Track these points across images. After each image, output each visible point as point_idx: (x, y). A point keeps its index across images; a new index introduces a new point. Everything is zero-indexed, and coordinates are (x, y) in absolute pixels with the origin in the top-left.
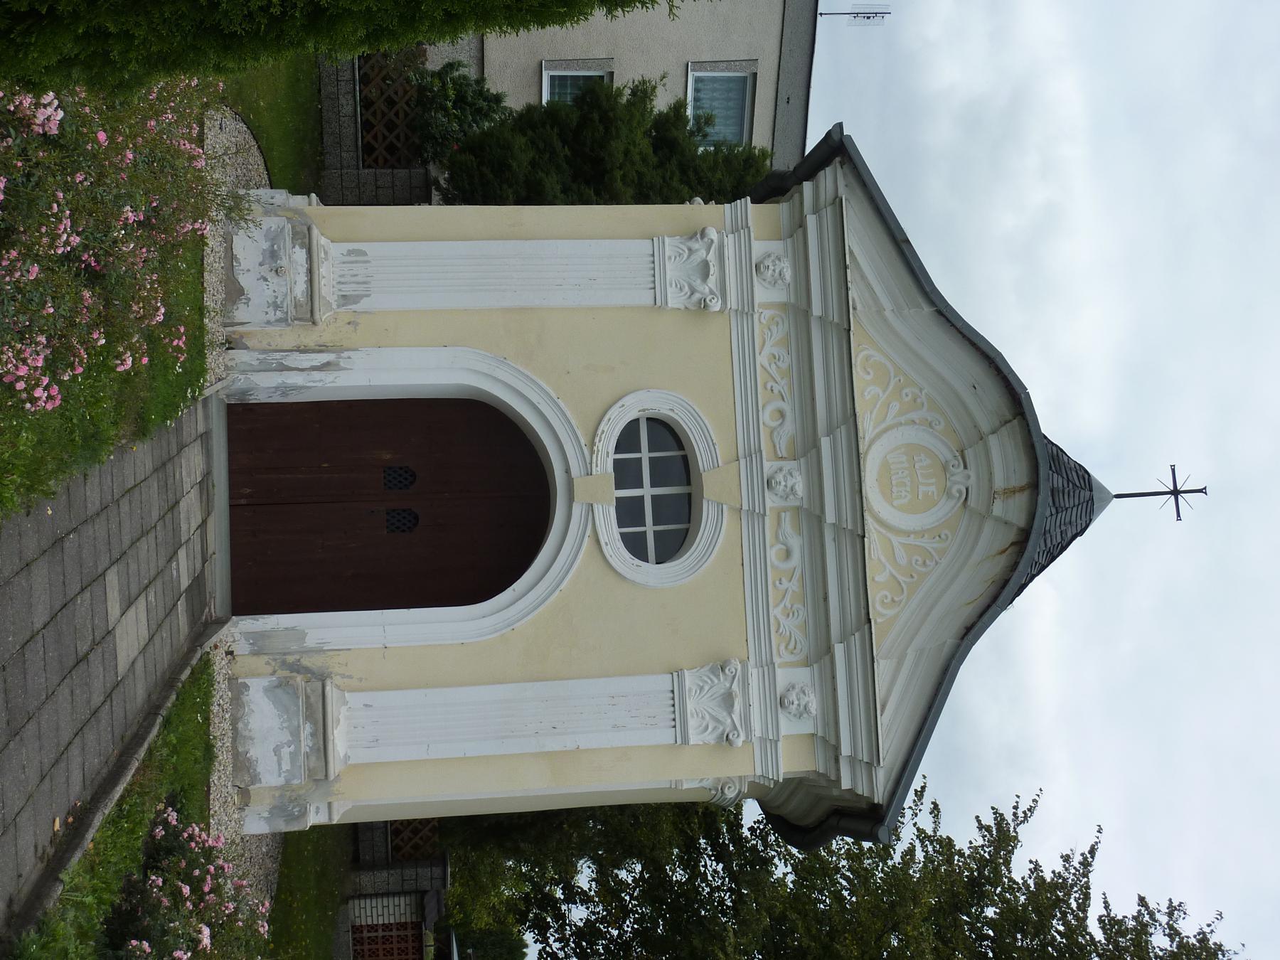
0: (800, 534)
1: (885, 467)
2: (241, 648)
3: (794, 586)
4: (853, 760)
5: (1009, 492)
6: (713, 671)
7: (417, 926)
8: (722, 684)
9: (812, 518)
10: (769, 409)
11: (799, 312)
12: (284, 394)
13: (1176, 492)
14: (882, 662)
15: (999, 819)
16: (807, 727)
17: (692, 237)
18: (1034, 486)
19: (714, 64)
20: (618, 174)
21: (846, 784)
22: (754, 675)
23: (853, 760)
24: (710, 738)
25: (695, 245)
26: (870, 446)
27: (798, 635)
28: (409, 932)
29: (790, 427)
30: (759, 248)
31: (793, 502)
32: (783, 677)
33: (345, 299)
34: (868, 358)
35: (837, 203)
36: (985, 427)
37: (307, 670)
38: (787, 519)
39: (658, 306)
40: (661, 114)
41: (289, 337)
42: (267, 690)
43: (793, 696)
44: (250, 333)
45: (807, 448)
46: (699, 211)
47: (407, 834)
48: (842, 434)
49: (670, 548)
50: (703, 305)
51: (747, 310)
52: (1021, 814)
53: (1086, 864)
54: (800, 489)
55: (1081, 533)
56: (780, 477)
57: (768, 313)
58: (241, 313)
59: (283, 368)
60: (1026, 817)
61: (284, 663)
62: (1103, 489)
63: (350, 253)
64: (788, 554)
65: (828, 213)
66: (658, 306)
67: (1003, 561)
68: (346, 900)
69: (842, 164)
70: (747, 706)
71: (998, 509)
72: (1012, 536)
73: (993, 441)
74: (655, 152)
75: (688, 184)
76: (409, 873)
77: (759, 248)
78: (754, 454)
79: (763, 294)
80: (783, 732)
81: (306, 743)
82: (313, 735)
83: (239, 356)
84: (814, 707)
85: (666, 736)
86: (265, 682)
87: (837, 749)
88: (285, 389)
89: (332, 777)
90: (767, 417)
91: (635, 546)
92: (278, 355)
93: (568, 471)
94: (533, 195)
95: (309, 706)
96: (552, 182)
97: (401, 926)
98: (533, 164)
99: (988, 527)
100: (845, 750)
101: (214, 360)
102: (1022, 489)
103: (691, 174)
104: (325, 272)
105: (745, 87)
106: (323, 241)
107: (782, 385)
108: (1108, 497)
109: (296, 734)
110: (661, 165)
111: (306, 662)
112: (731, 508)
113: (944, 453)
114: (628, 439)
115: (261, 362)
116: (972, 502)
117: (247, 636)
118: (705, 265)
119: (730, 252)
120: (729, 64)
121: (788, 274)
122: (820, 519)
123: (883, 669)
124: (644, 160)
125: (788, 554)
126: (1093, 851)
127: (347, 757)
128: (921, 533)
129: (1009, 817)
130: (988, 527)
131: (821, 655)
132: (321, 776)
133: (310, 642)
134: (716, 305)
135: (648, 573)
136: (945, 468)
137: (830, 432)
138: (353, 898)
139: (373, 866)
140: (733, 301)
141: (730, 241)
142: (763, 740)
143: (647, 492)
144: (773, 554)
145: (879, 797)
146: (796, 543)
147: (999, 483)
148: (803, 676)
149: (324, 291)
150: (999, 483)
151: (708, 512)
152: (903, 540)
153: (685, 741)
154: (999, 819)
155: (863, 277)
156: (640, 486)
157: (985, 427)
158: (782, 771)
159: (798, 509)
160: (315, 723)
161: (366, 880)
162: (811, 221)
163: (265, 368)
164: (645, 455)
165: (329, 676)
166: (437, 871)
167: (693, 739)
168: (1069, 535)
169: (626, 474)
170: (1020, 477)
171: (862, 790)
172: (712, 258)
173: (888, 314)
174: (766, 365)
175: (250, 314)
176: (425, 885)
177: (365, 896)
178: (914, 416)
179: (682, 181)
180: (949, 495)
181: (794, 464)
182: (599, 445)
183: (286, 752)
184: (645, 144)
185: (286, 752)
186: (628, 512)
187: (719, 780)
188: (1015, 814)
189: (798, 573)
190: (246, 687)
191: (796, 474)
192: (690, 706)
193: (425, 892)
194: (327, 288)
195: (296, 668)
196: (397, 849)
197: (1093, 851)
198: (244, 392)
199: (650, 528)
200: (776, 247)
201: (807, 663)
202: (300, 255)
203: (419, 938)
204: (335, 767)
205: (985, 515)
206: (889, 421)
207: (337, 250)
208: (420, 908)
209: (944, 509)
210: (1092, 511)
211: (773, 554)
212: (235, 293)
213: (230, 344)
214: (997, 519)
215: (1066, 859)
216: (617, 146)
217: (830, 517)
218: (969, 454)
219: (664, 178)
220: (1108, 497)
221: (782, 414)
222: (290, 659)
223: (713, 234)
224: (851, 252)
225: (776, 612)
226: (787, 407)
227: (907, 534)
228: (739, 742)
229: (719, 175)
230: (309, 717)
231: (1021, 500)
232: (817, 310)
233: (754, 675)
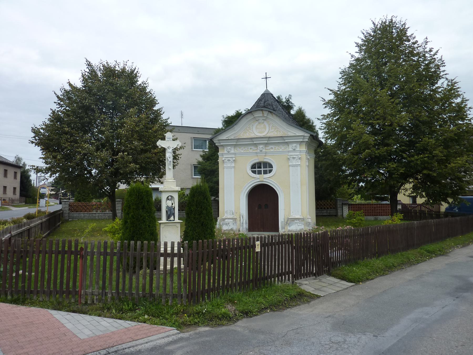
0: (269, 146)
1: (259, 133)
2: (284, 230)
3: (277, 147)
4: (303, 139)
5: (263, 114)
6: (289, 160)
7: (349, 205)
9: (266, 144)
10: (250, 150)
11: (235, 146)
12: (247, 223)
13: (266, 78)
15: (324, 104)
16: (298, 146)
18: (262, 110)
19: (192, 145)
20: (213, 168)
21: (307, 140)
22: (290, 154)
23: (303, 139)
24: (299, 161)
25: (225, 162)
27: (284, 147)
28: (350, 206)
29: (253, 147)
30: (226, 152)
32: (291, 149)
34: (242, 135)
36: (253, 117)
37: (287, 221)
38: (267, 148)
39: (234, 167)
40: (202, 159)
41: (238, 222)
42: (289, 227)
43: (293, 148)
44: (238, 228)
45: (256, 145)
46: (220, 160)
47: (318, 207)
48: (254, 140)
49: (271, 166)
50: (234, 160)
51: (235, 154)
52: (323, 100)
53: (331, 90)
54: (262, 146)
55: (272, 95)
56: (260, 149)
57: (235, 150)
58: (235, 229)
59: (243, 223)
60: (324, 99)
62: (265, 91)
63: (226, 213)
64: (272, 148)
65: (220, 141)
66: (234, 167)
67: (273, 115)
68: (343, 218)
70: (295, 155)
71: (266, 115)
72: (270, 113)
73: (255, 116)
74: (209, 161)
75: (215, 155)
76: (338, 206)
77: (226, 152)
78: (256, 153)
79: (232, 152)
80: (299, 150)
81: (298, 221)
82: (296, 220)
83: (241, 229)
84: (295, 145)
85: (299, 168)
86: (288, 227)
87: (301, 141)
88: (246, 223)
89: (303, 218)
90: (251, 151)
91: (270, 171)
93: (259, 182)
94: (217, 183)
95: (292, 221)
96: (215, 179)
97: (349, 208)
98: (211, 182)
99: (268, 117)
100: (302, 140)
101: (241, 232)
102: (263, 112)
103: (213, 155)
104: (229, 217)
105: (195, 139)
106: (224, 217)
107: (246, 148)
108: (267, 90)
109: (296, 223)
110: (211, 160)
111: (286, 221)
112: (265, 157)
113: (257, 123)
114: (254, 172)
115: (242, 226)
116: (265, 119)
117: (282, 230)
118: (228, 160)
119: (226, 156)
120: (192, 143)
121: (230, 147)
122: (267, 143)
124: (210, 163)
125: (272, 148)
126: (329, 89)
127: (300, 216)
128: (269, 127)
129: (324, 102)
130: (268, 117)
131: (287, 143)
132: (303, 219)
133: (283, 220)
134: (234, 159)
135: (274, 169)
136: (259, 123)
137: (253, 141)
138: (343, 216)
139: (337, 212)
140: (233, 156)
141: (225, 156)
142: (300, 152)
143: (262, 169)
144: (272, 150)
145: (309, 135)
146: (270, 147)
147: (262, 115)
148: (290, 146)
149: (232, 217)
150: (262, 115)
151: (265, 160)
152: (270, 130)
153: (300, 165)
154: (324, 104)
155: (230, 136)
157: (253, 117)
158: (305, 150)
159: (265, 146)
160: (295, 220)
161: (340, 214)
162: (221, 144)
163: (243, 226)
164: (257, 169)
165: (288, 218)
166: (338, 201)
167: (299, 163)
168: (273, 98)
169: (260, 173)
170: (261, 112)
171: (308, 138)
172: (227, 159)
173: (235, 132)
175: (235, 228)
176: (341, 203)
177: (343, 214)
178: (251, 128)
179: (214, 156)
180: (264, 122)
181: (258, 147)
182: (255, 177)
183: (299, 224)
184: (208, 163)
185: (299, 224)
186: (265, 172)
187: (306, 159)
188: (324, 101)
189: (275, 147)
190: (289, 230)
191: (260, 147)
192: (295, 164)
193: (342, 204)
194: (231, 216)
195: (287, 223)
196: (334, 208)
197: (329, 89)
198: (246, 229)
199: (268, 169)
200: (225, 149)
201: (289, 145)
202: (226, 220)
203: (352, 205)
204: (301, 217)
205: (267, 117)
206: (252, 132)
207: (226, 215)
208: (345, 204)
209: (265, 123)
210: (269, 93)
211: (272, 150)
212: (232, 230)
213: (239, 231)
214: (267, 115)
215: (330, 94)
216: (208, 168)
217: (266, 142)
218: (257, 119)
219: (213, 160)
220: (267, 90)
221: (251, 148)
222: (285, 223)
223: (223, 159)
226: (250, 148)
227: (269, 129)
228: (300, 156)
229: (213, 150)
231: (264, 112)
232: (235, 143)
233: (290, 154)
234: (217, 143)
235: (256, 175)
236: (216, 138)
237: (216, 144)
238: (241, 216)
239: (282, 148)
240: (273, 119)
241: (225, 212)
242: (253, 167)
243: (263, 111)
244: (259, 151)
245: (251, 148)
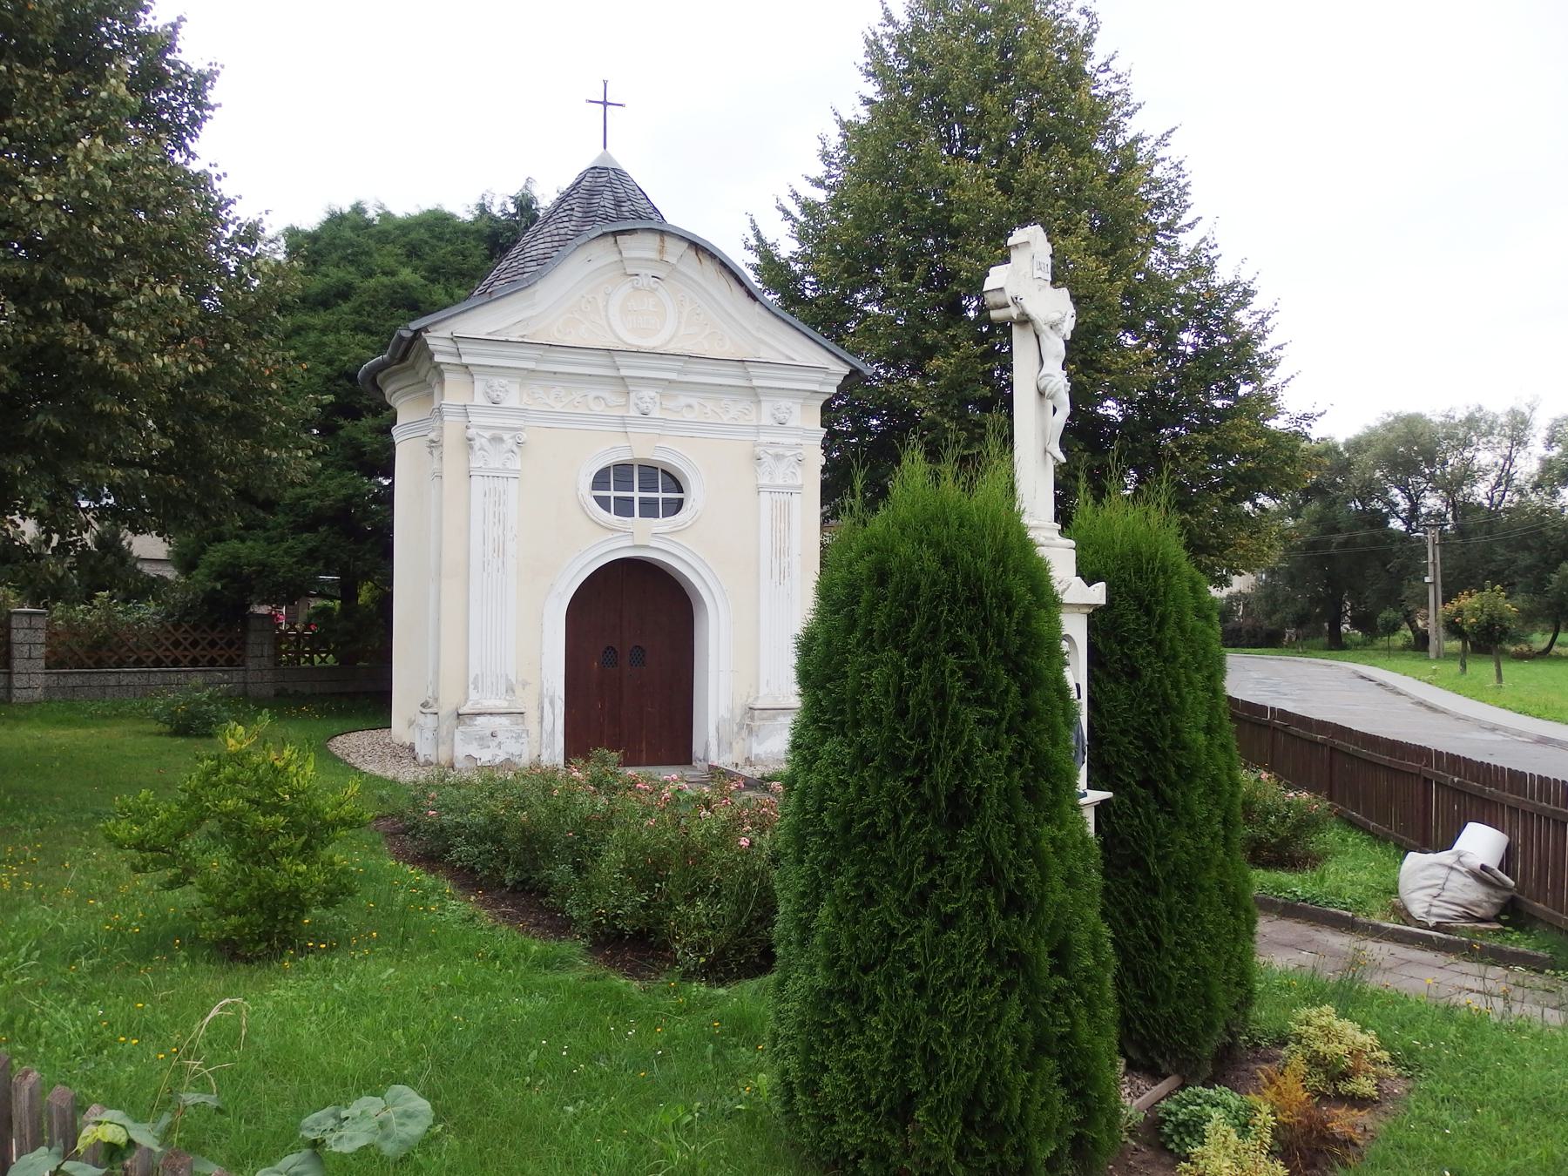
5: (661, 251)
6: (759, 466)
8: (767, 459)
13: (605, 103)
14: (761, 354)
16: (797, 409)
17: (471, 447)
23: (822, 383)
24: (799, 471)
25: (476, 447)
26: (620, 339)
31: (657, 399)
33: (510, 689)
34: (559, 331)
35: (454, 339)
38: (666, 404)
42: (759, 744)
48: (619, 360)
51: (522, 412)
61: (738, 733)
63: (476, 688)
64: (690, 406)
69: (427, 331)
71: (673, 260)
90: (598, 408)
91: (675, 507)
92: (544, 736)
102: (662, 241)
104: (491, 703)
106: (469, 703)
108: (605, 155)
121: (504, 381)
123: (766, 355)
125: (690, 406)
131: (755, 393)
133: (727, 716)
144: (689, 416)
145: (846, 370)
146: (683, 400)
147: (654, 255)
148: (767, 407)
149: (505, 704)
156: (632, 499)
164: (612, 494)
169: (624, 508)
172: (488, 434)
174: (561, 404)
181: (632, 395)
186: (649, 508)
189: (702, 401)
191: (641, 395)
194: (501, 704)
202: (480, 720)
207: (473, 695)
218: (629, 271)
220: (605, 155)
221: (597, 398)
222: (735, 729)
224: (489, 334)
225: (725, 419)
230: (774, 718)
233: (764, 439)
234: (442, 353)
235: (605, 513)
236: (437, 327)
237: (437, 358)
238: (546, 701)
239: (733, 411)
240: (697, 277)
241: (471, 679)
242: (600, 480)
243: (666, 238)
244: (634, 412)
245: (597, 398)
